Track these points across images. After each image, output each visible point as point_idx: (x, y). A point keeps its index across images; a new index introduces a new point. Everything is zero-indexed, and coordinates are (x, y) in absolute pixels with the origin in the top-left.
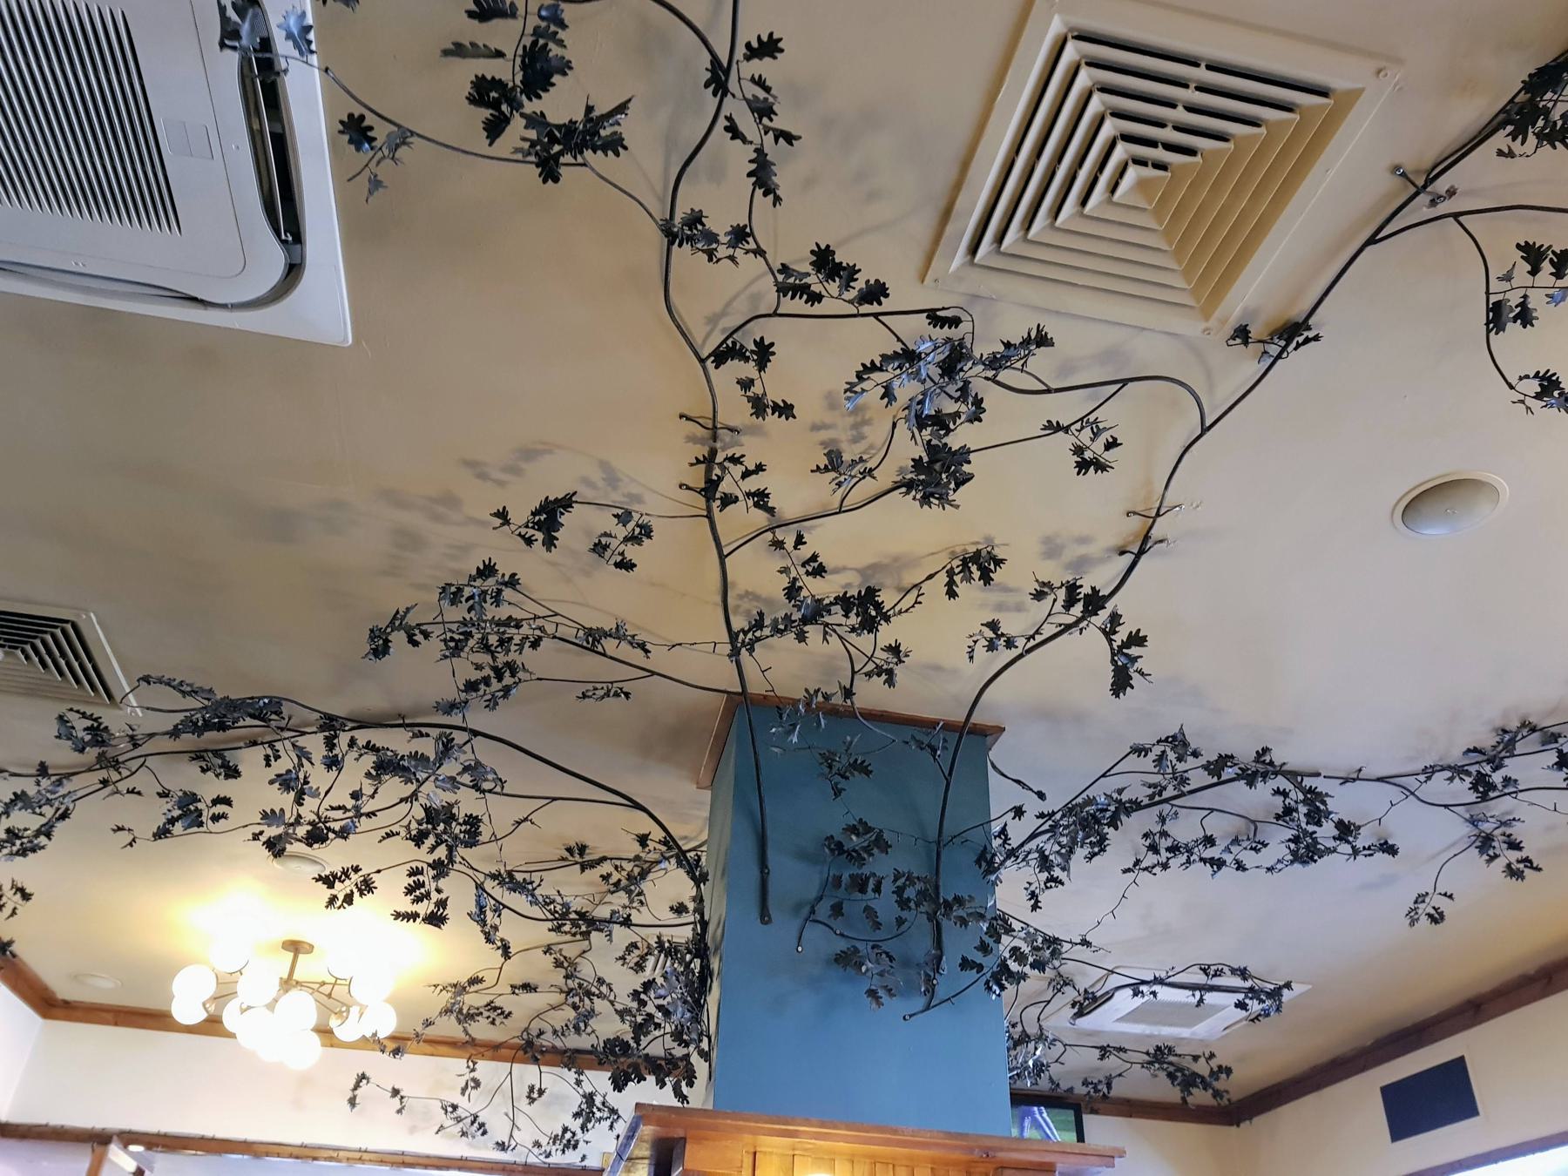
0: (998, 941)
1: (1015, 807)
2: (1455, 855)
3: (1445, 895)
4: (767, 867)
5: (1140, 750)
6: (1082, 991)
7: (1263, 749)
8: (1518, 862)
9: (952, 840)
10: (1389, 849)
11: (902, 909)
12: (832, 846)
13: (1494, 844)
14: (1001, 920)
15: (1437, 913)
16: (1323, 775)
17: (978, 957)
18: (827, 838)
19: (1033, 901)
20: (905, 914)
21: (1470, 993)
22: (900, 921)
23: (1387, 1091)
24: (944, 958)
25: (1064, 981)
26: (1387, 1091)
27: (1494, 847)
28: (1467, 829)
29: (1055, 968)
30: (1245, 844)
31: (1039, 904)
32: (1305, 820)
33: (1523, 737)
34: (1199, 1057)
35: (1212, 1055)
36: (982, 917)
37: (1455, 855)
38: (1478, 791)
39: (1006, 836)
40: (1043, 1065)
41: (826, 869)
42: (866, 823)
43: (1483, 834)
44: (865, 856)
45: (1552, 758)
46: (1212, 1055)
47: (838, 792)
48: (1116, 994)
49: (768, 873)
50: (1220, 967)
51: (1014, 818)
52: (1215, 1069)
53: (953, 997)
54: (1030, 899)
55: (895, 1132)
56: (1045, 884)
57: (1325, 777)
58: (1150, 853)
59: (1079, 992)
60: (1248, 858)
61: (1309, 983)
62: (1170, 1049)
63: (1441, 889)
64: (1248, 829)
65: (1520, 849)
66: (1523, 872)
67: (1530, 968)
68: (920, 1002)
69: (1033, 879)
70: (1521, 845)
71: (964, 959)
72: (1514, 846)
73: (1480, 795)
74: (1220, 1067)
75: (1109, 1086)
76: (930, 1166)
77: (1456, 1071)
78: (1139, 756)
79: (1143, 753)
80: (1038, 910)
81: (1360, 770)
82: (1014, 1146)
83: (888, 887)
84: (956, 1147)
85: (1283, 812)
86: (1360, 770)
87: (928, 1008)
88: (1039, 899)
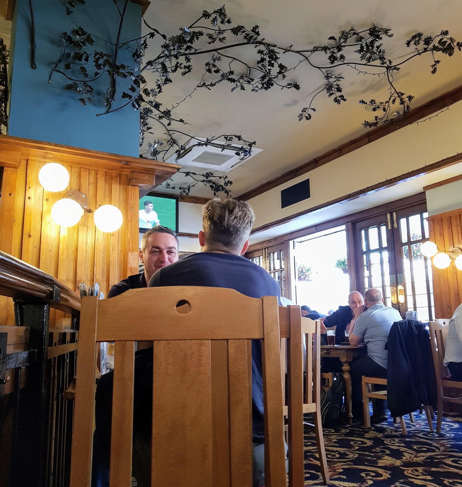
0: (139, 86)
1: (151, 33)
2: (319, 92)
3: (313, 109)
4: (34, 44)
5: (206, 15)
6: (180, 146)
7: (256, 26)
8: (339, 97)
9: (122, 45)
10: (297, 87)
11: (98, 69)
12: (66, 38)
13: (332, 89)
14: (140, 77)
15: (309, 116)
16: (277, 47)
17: (130, 93)
18: (63, 34)
19: (159, 89)
20: (99, 71)
21: (315, 156)
22: (97, 74)
23: (284, 193)
24: (116, 93)
25: (174, 142)
26: (284, 193)
27: (332, 90)
28: (325, 81)
29: (170, 135)
30: (245, 79)
31: (161, 90)
32: (268, 64)
33: (351, 37)
34: (222, 177)
35: (226, 177)
36: (132, 74)
37: (319, 92)
38: (331, 60)
39: (146, 44)
40: (157, 151)
41: (64, 49)
42: (82, 29)
43: (330, 84)
44: (82, 45)
45: (358, 48)
46: (226, 177)
47: (69, 13)
48: (193, 148)
49: (35, 47)
50: (232, 136)
51: (150, 38)
52: (227, 182)
53: (118, 109)
54: (158, 88)
55: (88, 151)
56: (164, 82)
57: (278, 48)
58: (208, 72)
59: (179, 146)
60: (246, 86)
61: (263, 149)
62: (212, 174)
63: (312, 107)
64: (247, 71)
65: (341, 91)
66: (340, 101)
67: (335, 147)
68: (104, 110)
69: (159, 78)
70: (341, 90)
71: (124, 93)
72: (339, 90)
73: (331, 61)
74: (228, 181)
75: (189, 189)
76: (104, 170)
77: (306, 184)
78: (206, 18)
79: (207, 17)
80: (161, 93)
81: (291, 46)
82: (137, 161)
83: (91, 59)
84: (114, 160)
85: (260, 60)
86: (291, 46)
87: (107, 112)
88: (161, 88)
